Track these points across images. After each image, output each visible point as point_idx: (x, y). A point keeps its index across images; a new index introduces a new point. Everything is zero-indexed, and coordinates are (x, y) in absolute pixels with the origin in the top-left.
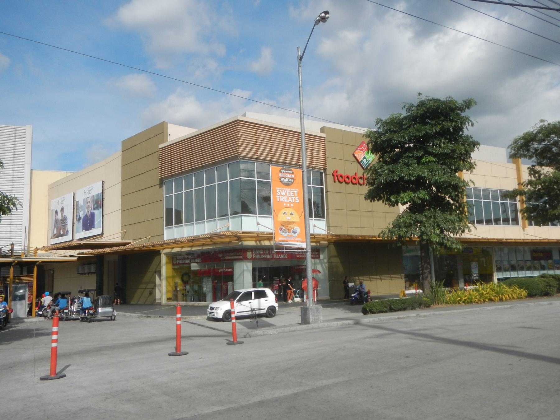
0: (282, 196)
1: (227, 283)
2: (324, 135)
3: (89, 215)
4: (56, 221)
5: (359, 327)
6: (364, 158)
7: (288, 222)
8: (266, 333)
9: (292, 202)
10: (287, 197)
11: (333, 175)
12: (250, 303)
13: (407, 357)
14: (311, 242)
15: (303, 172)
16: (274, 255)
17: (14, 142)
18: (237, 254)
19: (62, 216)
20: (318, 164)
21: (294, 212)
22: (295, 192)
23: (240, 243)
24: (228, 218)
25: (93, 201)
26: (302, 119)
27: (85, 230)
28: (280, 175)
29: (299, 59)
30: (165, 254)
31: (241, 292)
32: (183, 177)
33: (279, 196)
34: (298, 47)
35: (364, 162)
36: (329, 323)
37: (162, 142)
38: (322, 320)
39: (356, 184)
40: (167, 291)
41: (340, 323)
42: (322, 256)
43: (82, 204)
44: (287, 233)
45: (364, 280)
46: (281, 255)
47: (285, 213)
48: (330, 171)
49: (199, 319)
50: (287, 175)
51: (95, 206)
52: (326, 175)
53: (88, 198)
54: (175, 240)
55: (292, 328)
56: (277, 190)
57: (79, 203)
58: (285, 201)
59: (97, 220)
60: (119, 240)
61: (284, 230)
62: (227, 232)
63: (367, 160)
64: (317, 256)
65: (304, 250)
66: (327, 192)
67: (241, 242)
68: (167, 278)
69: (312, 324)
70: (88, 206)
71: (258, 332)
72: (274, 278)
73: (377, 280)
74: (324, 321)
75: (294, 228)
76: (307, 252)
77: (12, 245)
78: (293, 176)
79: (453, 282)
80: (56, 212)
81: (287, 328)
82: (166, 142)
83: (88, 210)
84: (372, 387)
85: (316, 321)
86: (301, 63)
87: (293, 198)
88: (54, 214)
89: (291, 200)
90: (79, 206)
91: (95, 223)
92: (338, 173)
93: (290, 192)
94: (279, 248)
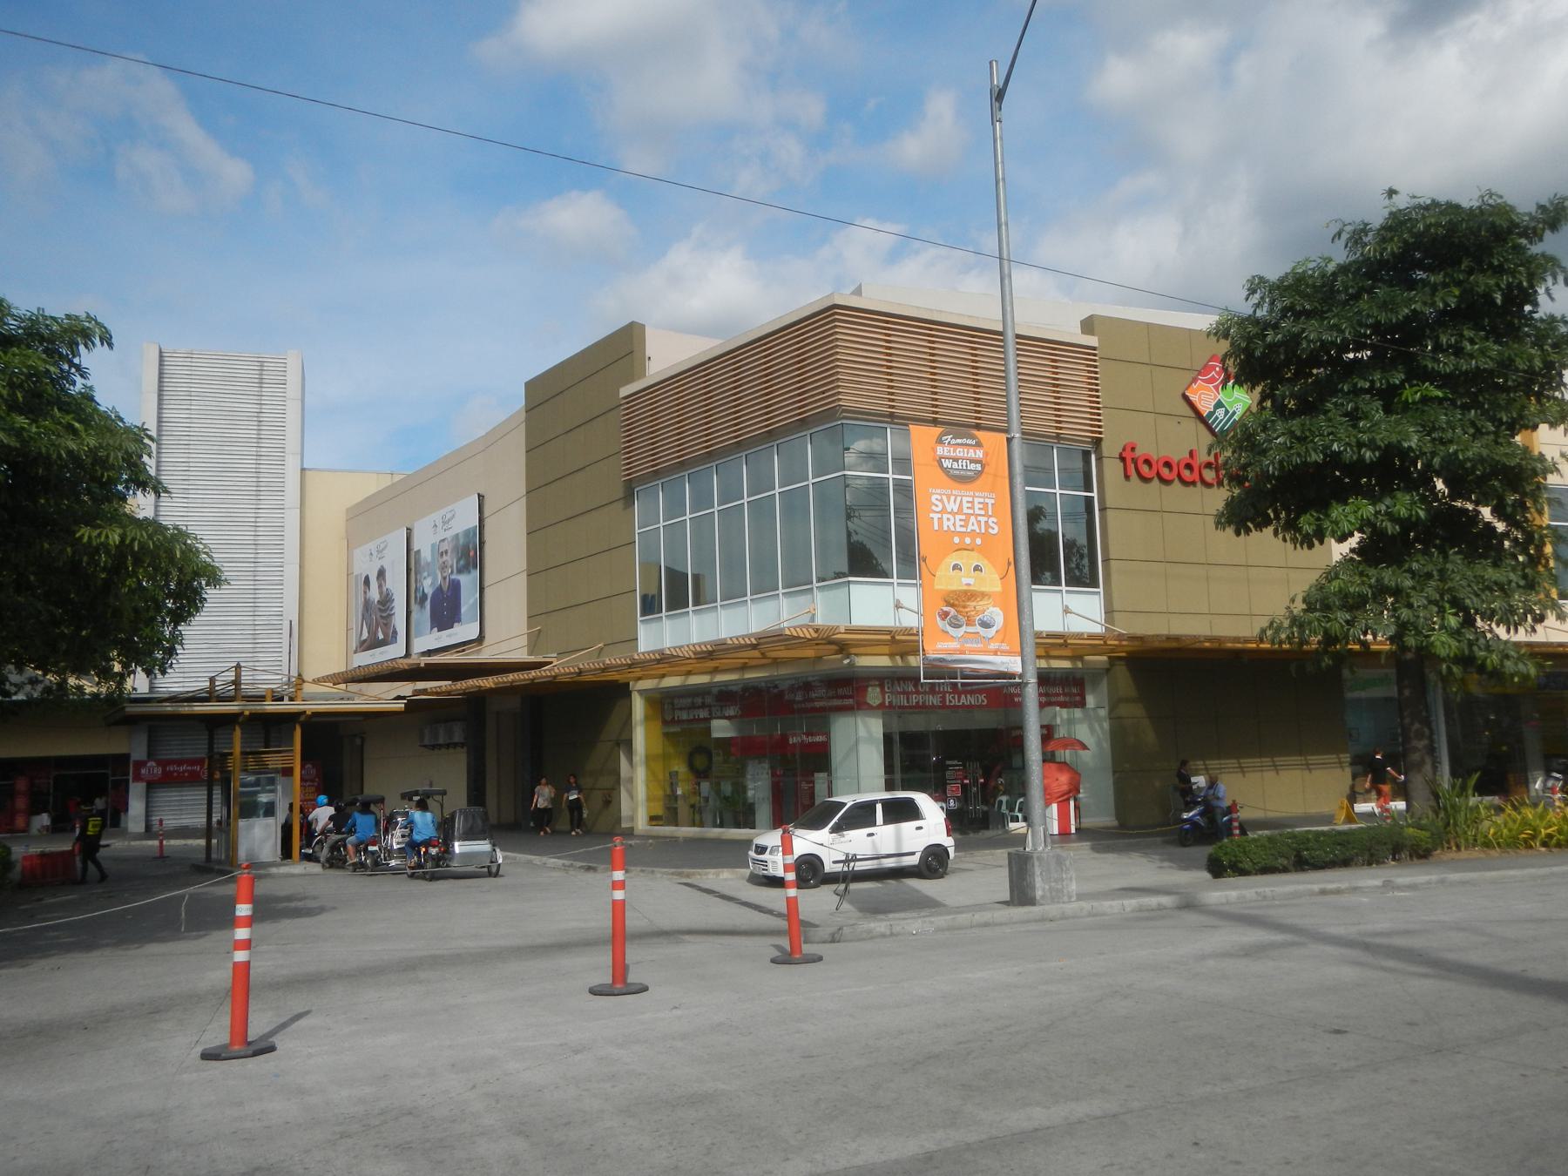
0: (950, 513)
1: (813, 776)
2: (1092, 341)
3: (445, 588)
4: (367, 604)
5: (1191, 918)
6: (1219, 405)
7: (966, 592)
8: (897, 929)
9: (978, 531)
10: (963, 517)
11: (1123, 459)
12: (870, 835)
13: (1338, 1032)
14: (1039, 657)
15: (1009, 440)
16: (947, 695)
17: (259, 398)
18: (840, 691)
19: (381, 593)
20: (1077, 428)
21: (983, 563)
22: (987, 500)
23: (846, 662)
24: (812, 588)
25: (456, 548)
26: (1007, 282)
27: (436, 629)
28: (940, 450)
29: (994, 100)
30: (641, 692)
31: (845, 804)
32: (687, 477)
33: (939, 516)
34: (991, 63)
35: (1217, 418)
36: (1095, 904)
37: (630, 379)
38: (1074, 893)
39: (1193, 483)
40: (649, 799)
41: (1131, 903)
42: (1091, 700)
43: (429, 559)
44: (964, 628)
45: (1223, 770)
46: (969, 696)
47: (956, 567)
48: (1111, 448)
49: (726, 880)
50: (960, 452)
51: (462, 562)
52: (1099, 459)
53: (443, 540)
54: (661, 652)
55: (979, 917)
56: (934, 498)
57: (423, 555)
58: (959, 529)
59: (468, 600)
60: (522, 655)
61: (955, 618)
62: (804, 629)
64: (1078, 698)
65: (1017, 680)
66: (1103, 509)
67: (848, 658)
68: (649, 759)
69: (1042, 905)
70: (444, 563)
71: (872, 925)
72: (948, 762)
73: (1262, 771)
74: (1080, 897)
75: (984, 612)
76: (1027, 684)
77: (238, 667)
78: (979, 454)
79: (1511, 778)
80: (367, 581)
81: (964, 915)
82: (639, 378)
83: (445, 575)
84: (1196, 1144)
85: (1056, 896)
86: (1000, 109)
87: (983, 519)
88: (361, 586)
89: (976, 527)
90: (422, 563)
91: (463, 610)
92: (1139, 452)
93: (972, 502)
94: (939, 670)
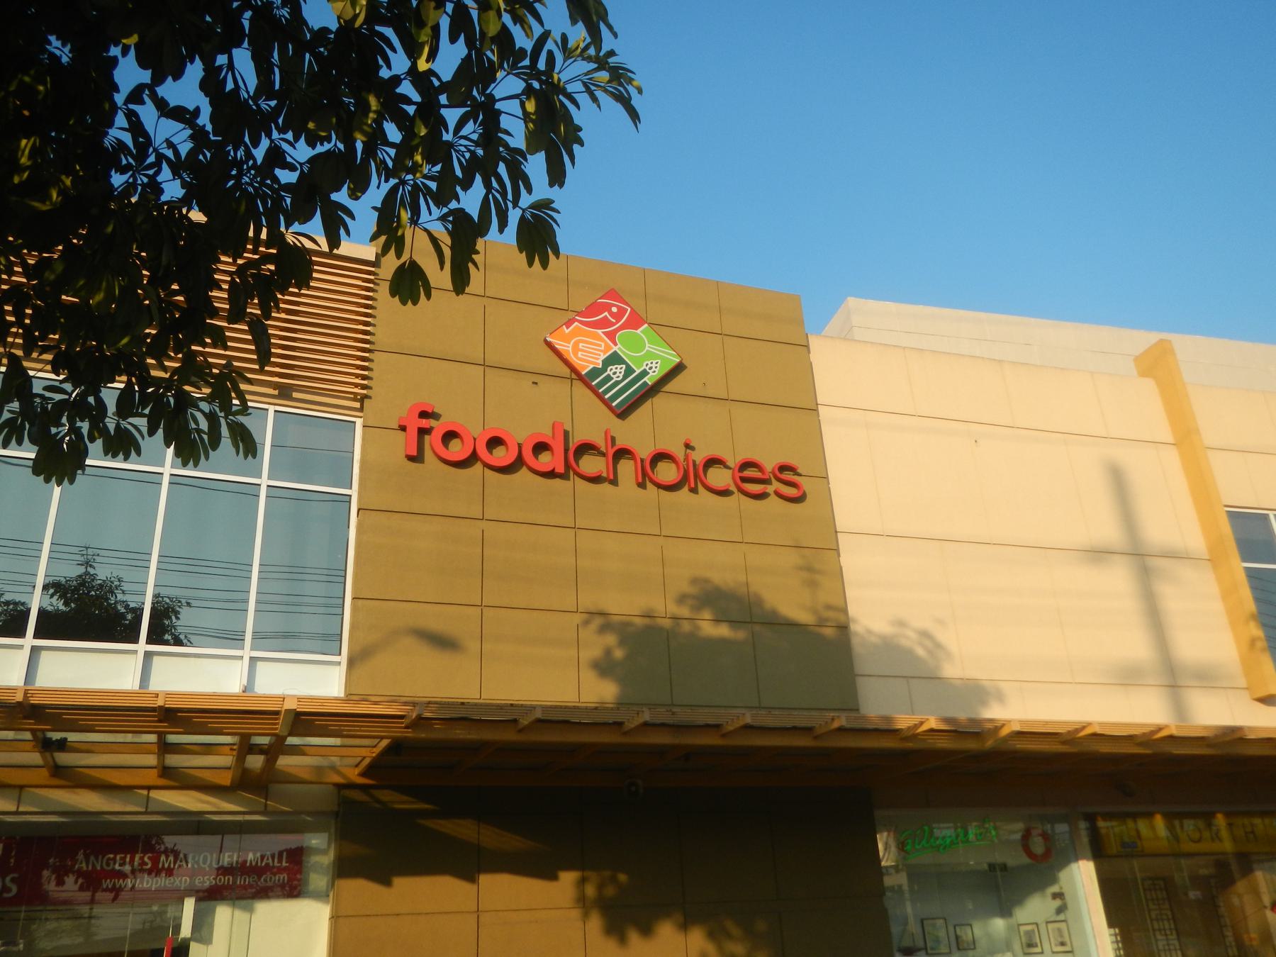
63: (628, 366)
